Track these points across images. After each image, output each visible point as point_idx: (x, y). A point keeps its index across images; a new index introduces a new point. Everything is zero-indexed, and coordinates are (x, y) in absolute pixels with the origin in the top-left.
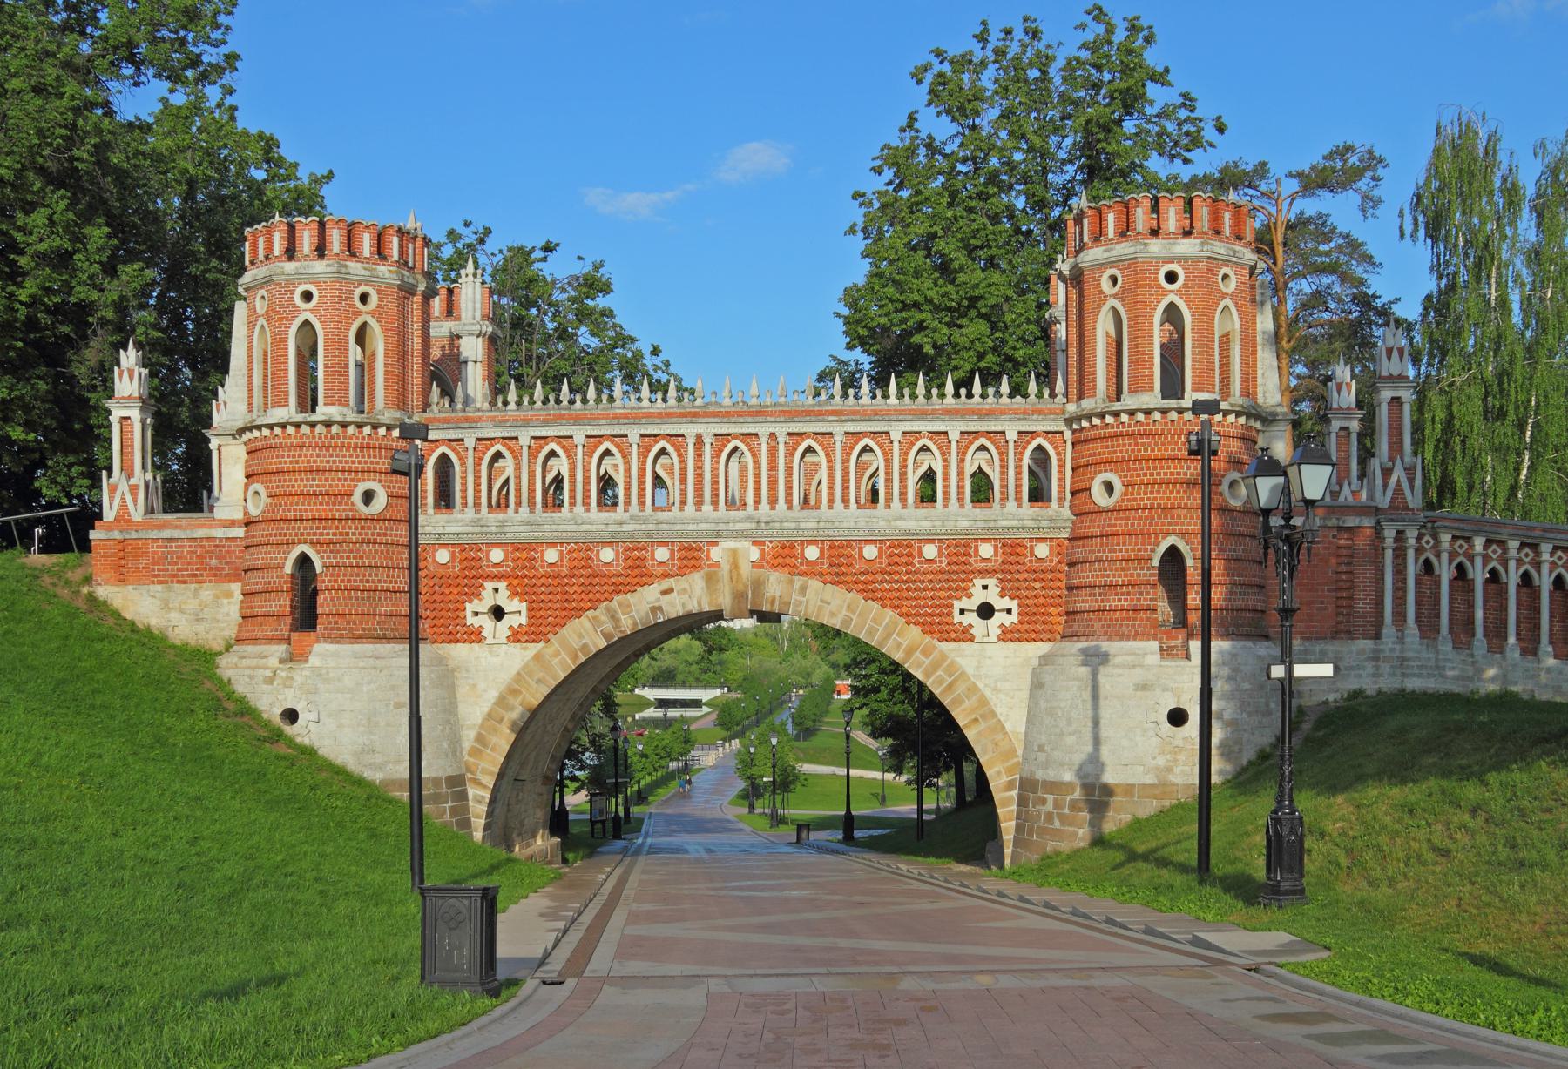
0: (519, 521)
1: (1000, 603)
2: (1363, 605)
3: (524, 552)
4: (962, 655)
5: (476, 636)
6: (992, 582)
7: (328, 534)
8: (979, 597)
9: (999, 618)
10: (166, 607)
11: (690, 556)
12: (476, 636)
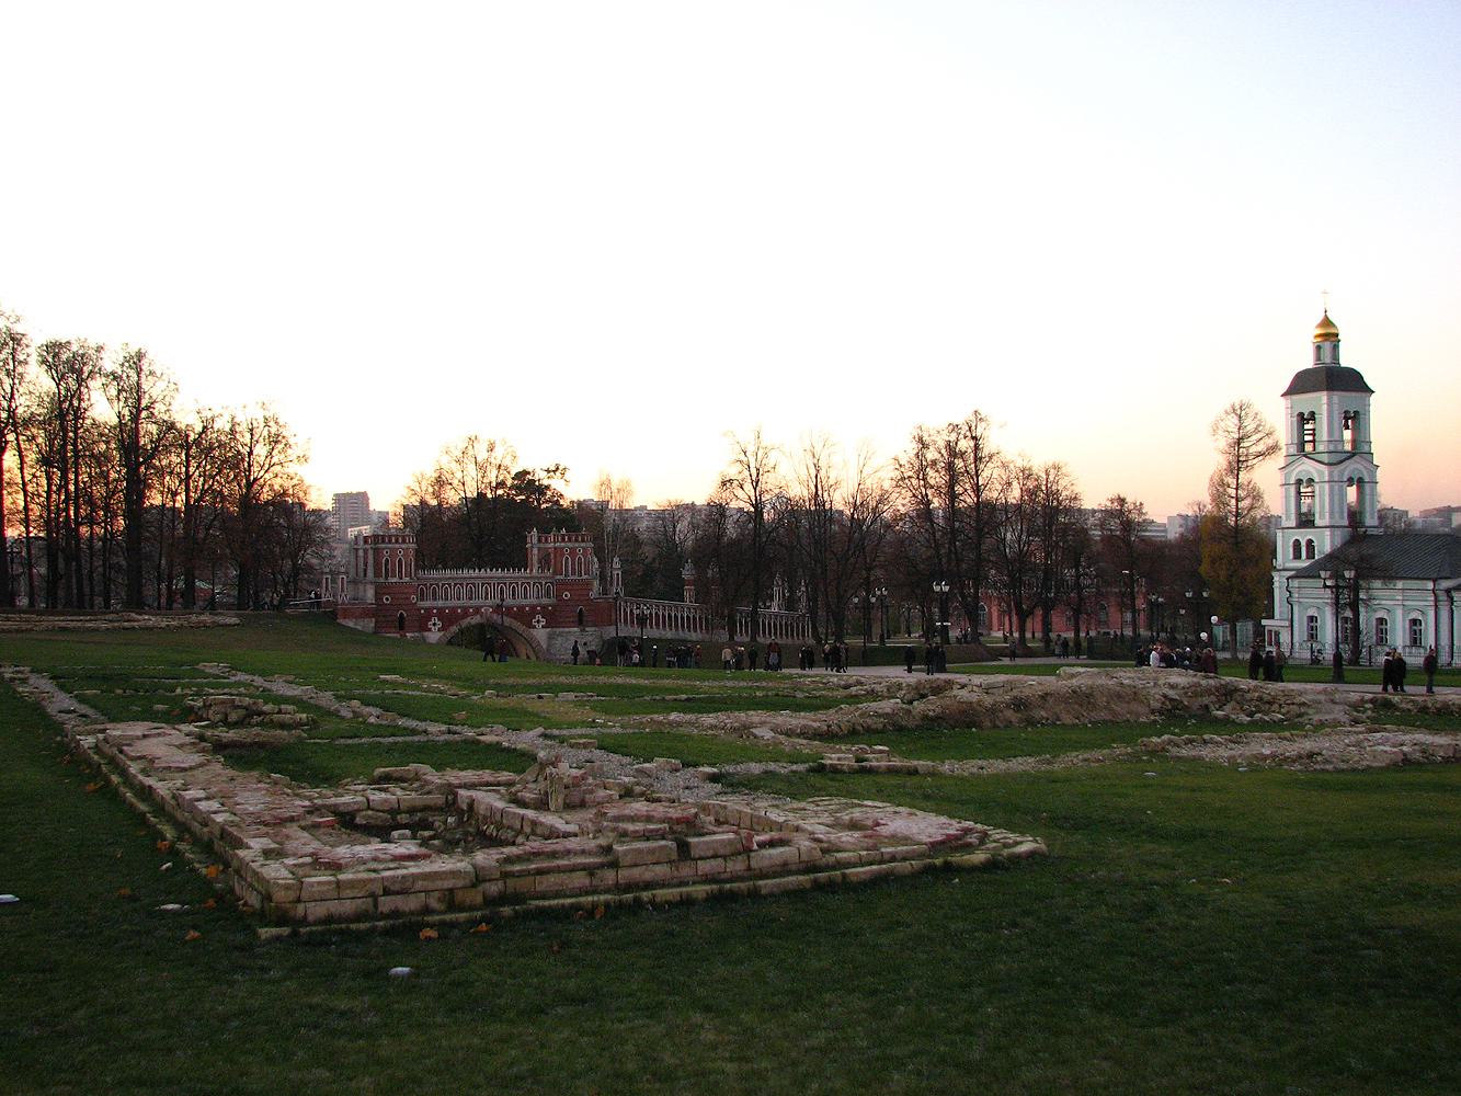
0: (440, 603)
2: (613, 618)
3: (441, 610)
4: (534, 632)
5: (430, 630)
7: (406, 608)
10: (356, 624)
11: (477, 610)
12: (430, 630)
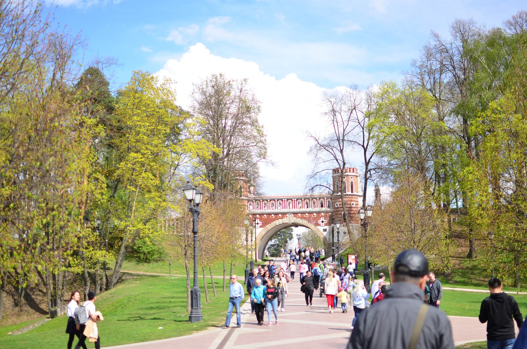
1: (324, 221)
6: (323, 218)
8: (322, 220)
9: (324, 223)
